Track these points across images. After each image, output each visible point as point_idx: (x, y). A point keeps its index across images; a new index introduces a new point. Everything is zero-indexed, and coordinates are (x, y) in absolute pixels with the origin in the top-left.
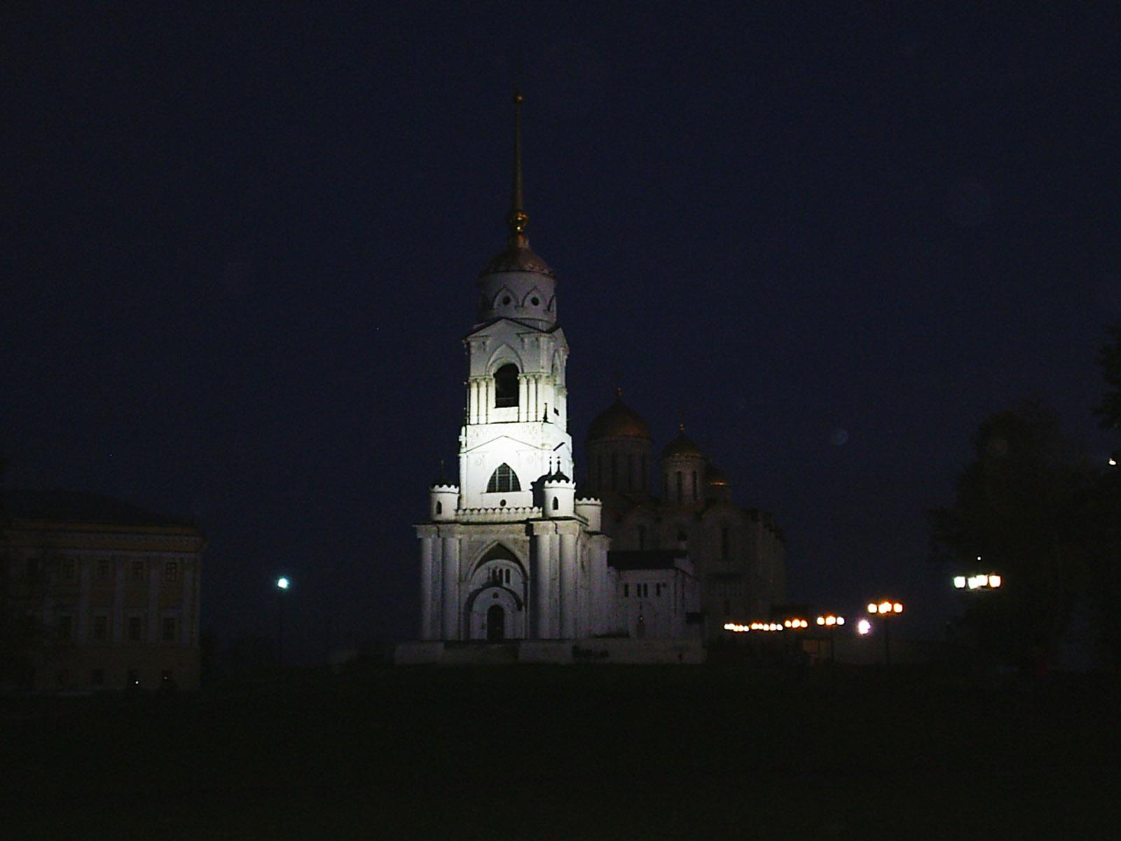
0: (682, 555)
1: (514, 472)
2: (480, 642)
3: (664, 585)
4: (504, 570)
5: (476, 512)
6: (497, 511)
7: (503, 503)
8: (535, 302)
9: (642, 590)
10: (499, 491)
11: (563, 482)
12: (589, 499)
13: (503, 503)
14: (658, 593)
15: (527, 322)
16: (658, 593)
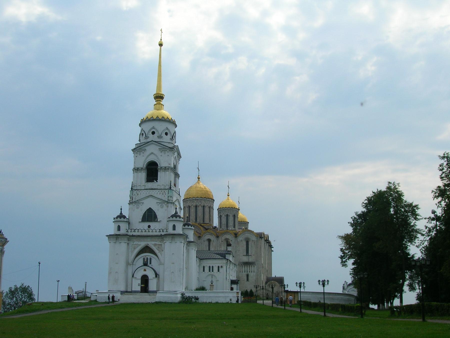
0: (229, 253)
1: (155, 212)
2: (136, 292)
3: (222, 267)
4: (149, 258)
5: (136, 231)
6: (147, 231)
7: (149, 227)
8: (166, 134)
9: (211, 269)
10: (148, 221)
11: (178, 219)
12: (188, 226)
13: (149, 227)
14: (218, 271)
15: (163, 143)
16: (218, 271)
